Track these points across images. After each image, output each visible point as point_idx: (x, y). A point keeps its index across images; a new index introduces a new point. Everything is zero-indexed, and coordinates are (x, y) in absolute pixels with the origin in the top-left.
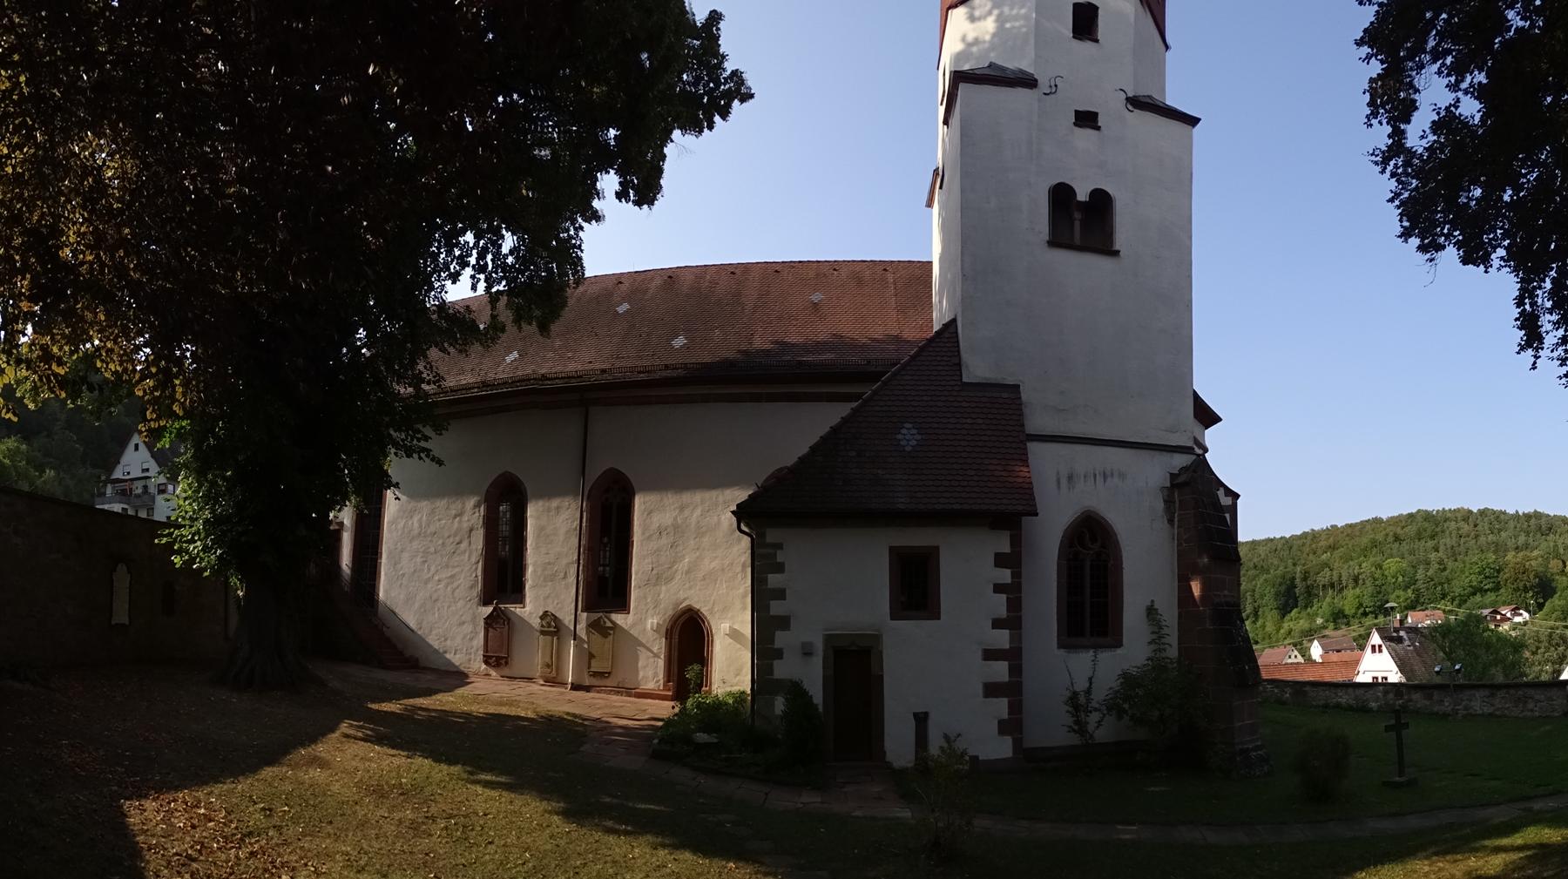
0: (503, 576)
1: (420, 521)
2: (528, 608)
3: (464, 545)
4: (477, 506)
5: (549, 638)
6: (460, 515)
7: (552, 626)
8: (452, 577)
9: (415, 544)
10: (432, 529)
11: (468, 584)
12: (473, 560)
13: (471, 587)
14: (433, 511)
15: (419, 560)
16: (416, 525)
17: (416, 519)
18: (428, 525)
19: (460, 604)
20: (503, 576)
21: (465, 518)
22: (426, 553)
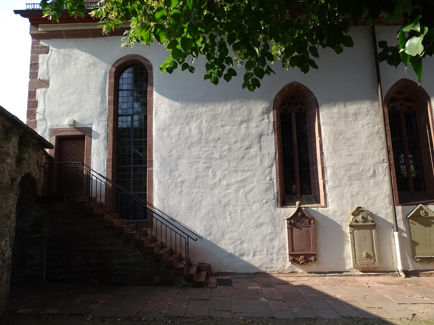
0: (297, 175)
1: (199, 127)
2: (331, 207)
3: (254, 150)
4: (266, 112)
5: (368, 231)
6: (248, 120)
7: (365, 222)
8: (242, 181)
9: (195, 151)
10: (215, 134)
11: (263, 187)
12: (266, 163)
13: (267, 190)
14: (214, 117)
15: (201, 165)
16: (194, 131)
17: (193, 125)
18: (210, 131)
19: (255, 207)
20: (297, 175)
21: (253, 124)
22: (209, 158)
